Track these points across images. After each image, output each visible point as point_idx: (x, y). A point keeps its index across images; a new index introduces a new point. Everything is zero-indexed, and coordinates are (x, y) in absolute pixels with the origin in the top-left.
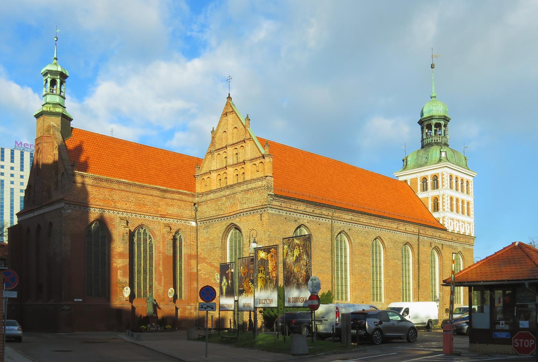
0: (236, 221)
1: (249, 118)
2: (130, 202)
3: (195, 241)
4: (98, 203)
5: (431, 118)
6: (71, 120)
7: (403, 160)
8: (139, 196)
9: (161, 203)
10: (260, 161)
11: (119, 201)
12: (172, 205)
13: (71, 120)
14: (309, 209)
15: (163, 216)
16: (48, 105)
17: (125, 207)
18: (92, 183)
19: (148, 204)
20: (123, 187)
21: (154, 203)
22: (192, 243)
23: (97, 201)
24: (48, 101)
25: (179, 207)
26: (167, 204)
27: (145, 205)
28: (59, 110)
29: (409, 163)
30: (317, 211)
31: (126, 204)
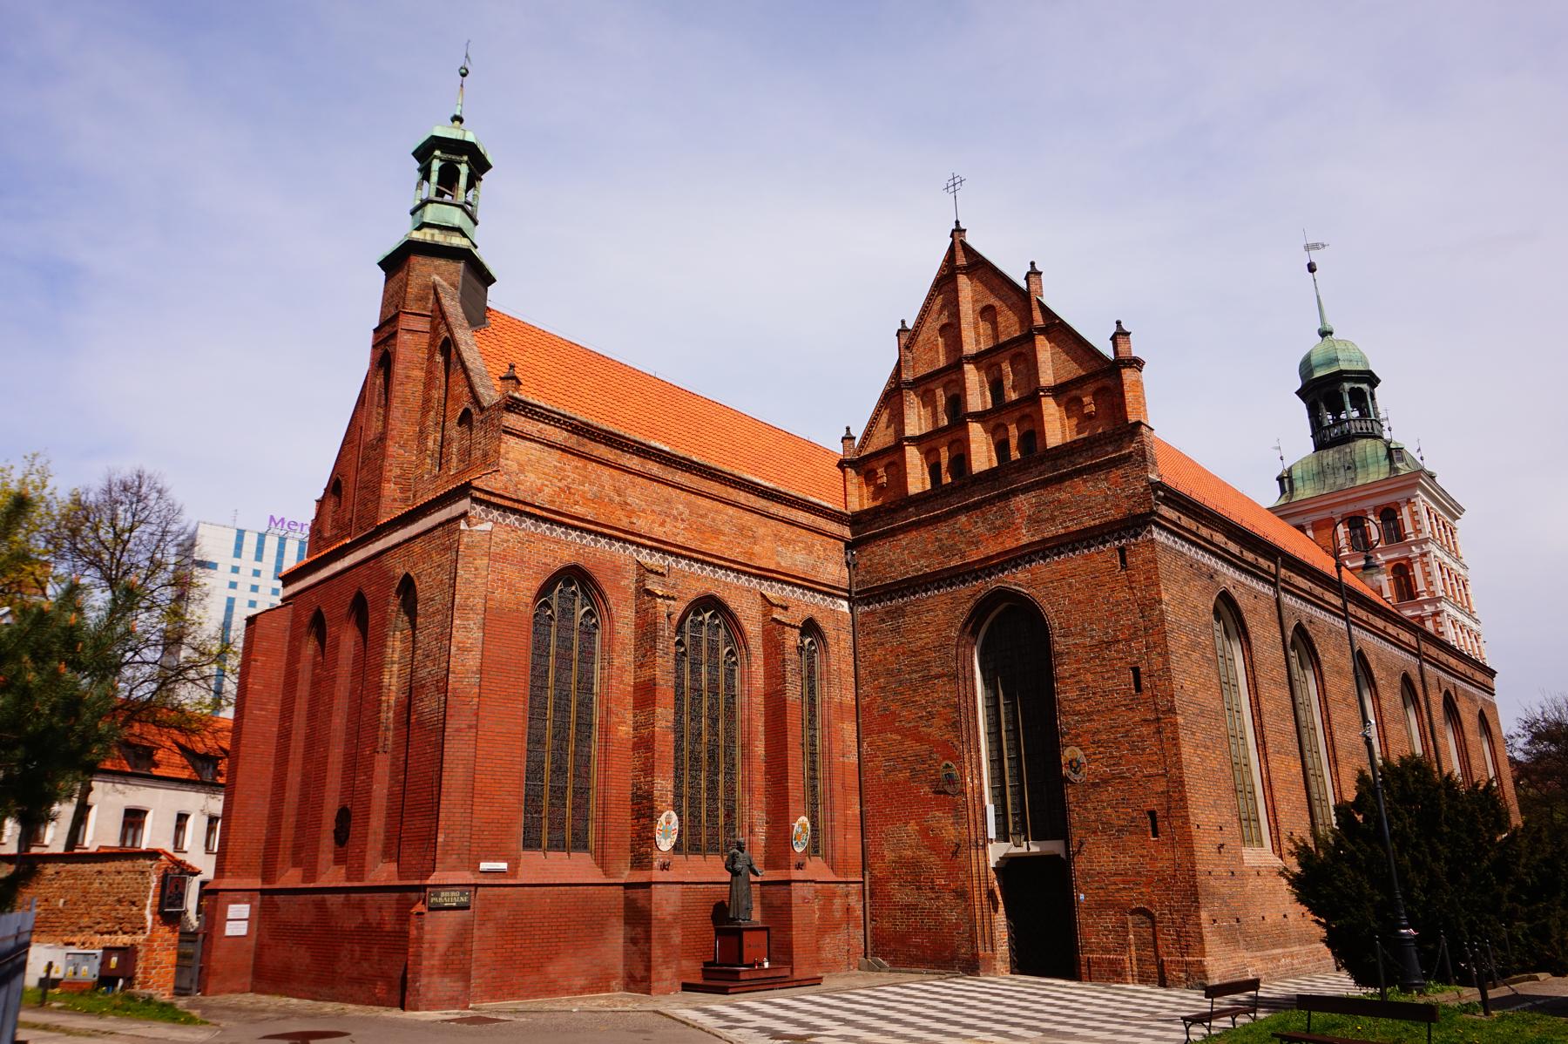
0: (1017, 579)
1: (1038, 268)
2: (675, 518)
3: (851, 659)
4: (579, 510)
5: (1341, 376)
6: (488, 279)
7: (1280, 479)
8: (701, 501)
9: (761, 531)
10: (1099, 384)
11: (643, 511)
12: (788, 542)
13: (488, 279)
14: (1233, 548)
15: (765, 575)
16: (426, 230)
17: (658, 532)
18: (565, 440)
19: (726, 529)
20: (654, 468)
21: (741, 530)
22: (843, 666)
23: (576, 503)
24: (427, 220)
25: (809, 549)
26: (778, 537)
27: (717, 533)
28: (457, 241)
29: (1298, 484)
30: (1249, 556)
31: (662, 524)
